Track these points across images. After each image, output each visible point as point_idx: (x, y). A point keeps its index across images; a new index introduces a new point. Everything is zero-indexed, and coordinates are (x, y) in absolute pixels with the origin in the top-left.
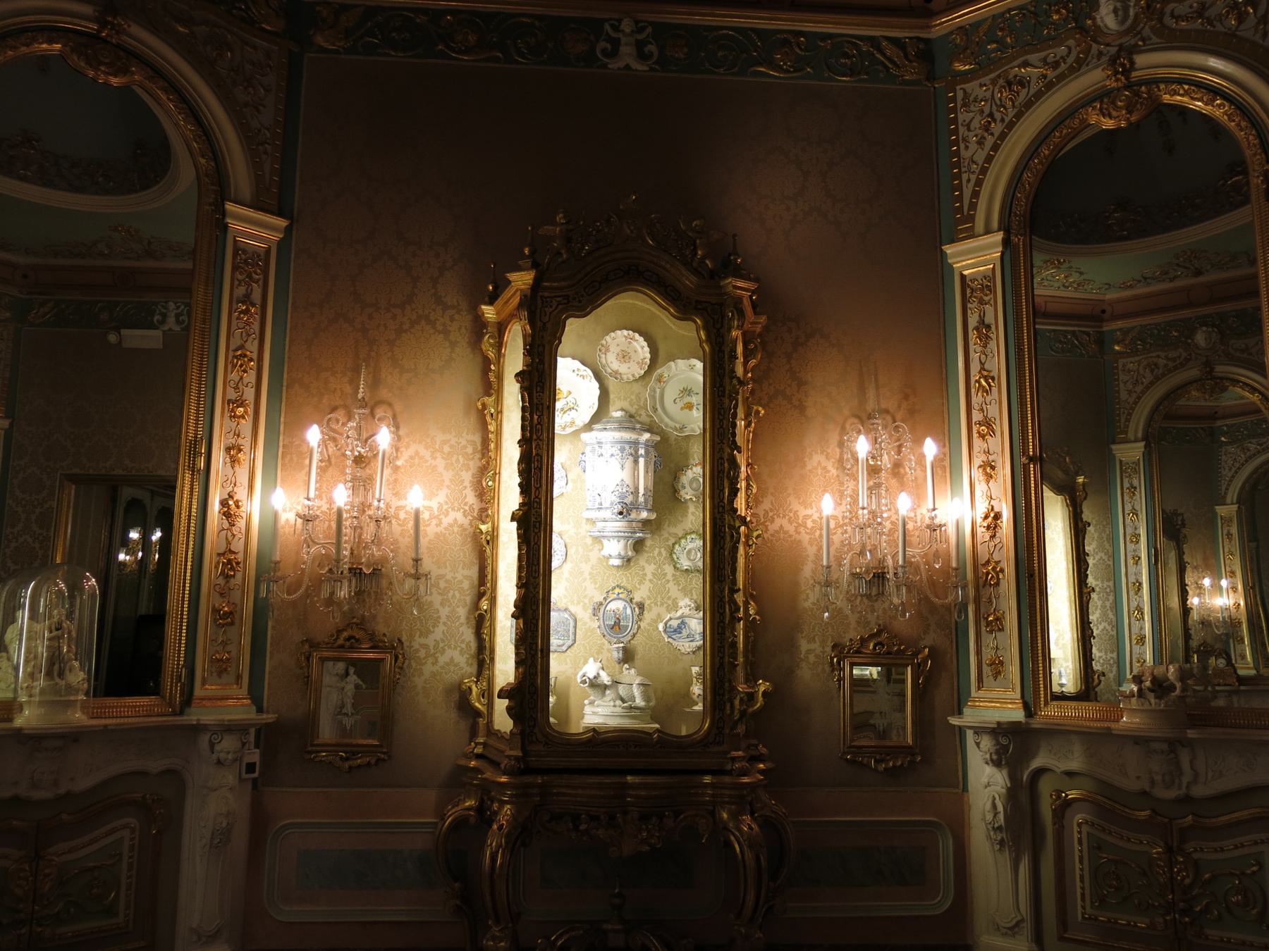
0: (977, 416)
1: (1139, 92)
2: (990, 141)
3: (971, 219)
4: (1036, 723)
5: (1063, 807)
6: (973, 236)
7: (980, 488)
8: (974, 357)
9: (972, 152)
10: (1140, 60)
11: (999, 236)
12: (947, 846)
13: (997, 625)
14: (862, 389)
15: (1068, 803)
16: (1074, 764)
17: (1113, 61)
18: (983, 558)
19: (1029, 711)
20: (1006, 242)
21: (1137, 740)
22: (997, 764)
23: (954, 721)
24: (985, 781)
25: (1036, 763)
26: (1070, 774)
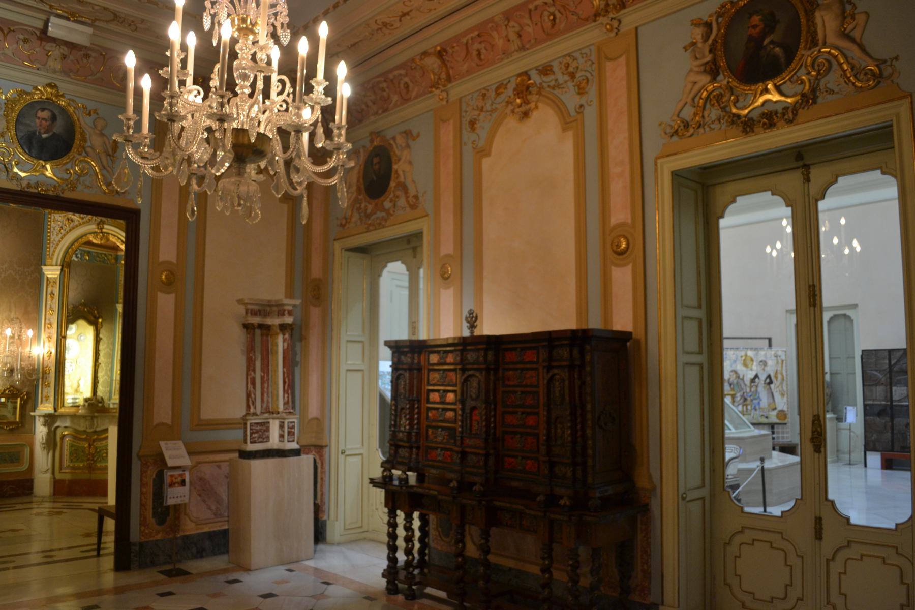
0: (47, 322)
1: (105, 235)
2: (60, 236)
3: (52, 259)
4: (57, 414)
5: (63, 436)
6: (52, 265)
7: (47, 344)
8: (49, 303)
9: (54, 237)
10: (106, 226)
11: (60, 268)
12: (27, 451)
13: (48, 385)
14: (10, 310)
15: (64, 435)
16: (67, 424)
17: (98, 224)
18: (45, 365)
19: (55, 410)
20: (62, 270)
21: (84, 417)
22: (44, 425)
23: (32, 414)
24: (41, 431)
25: (56, 425)
26: (66, 427)
